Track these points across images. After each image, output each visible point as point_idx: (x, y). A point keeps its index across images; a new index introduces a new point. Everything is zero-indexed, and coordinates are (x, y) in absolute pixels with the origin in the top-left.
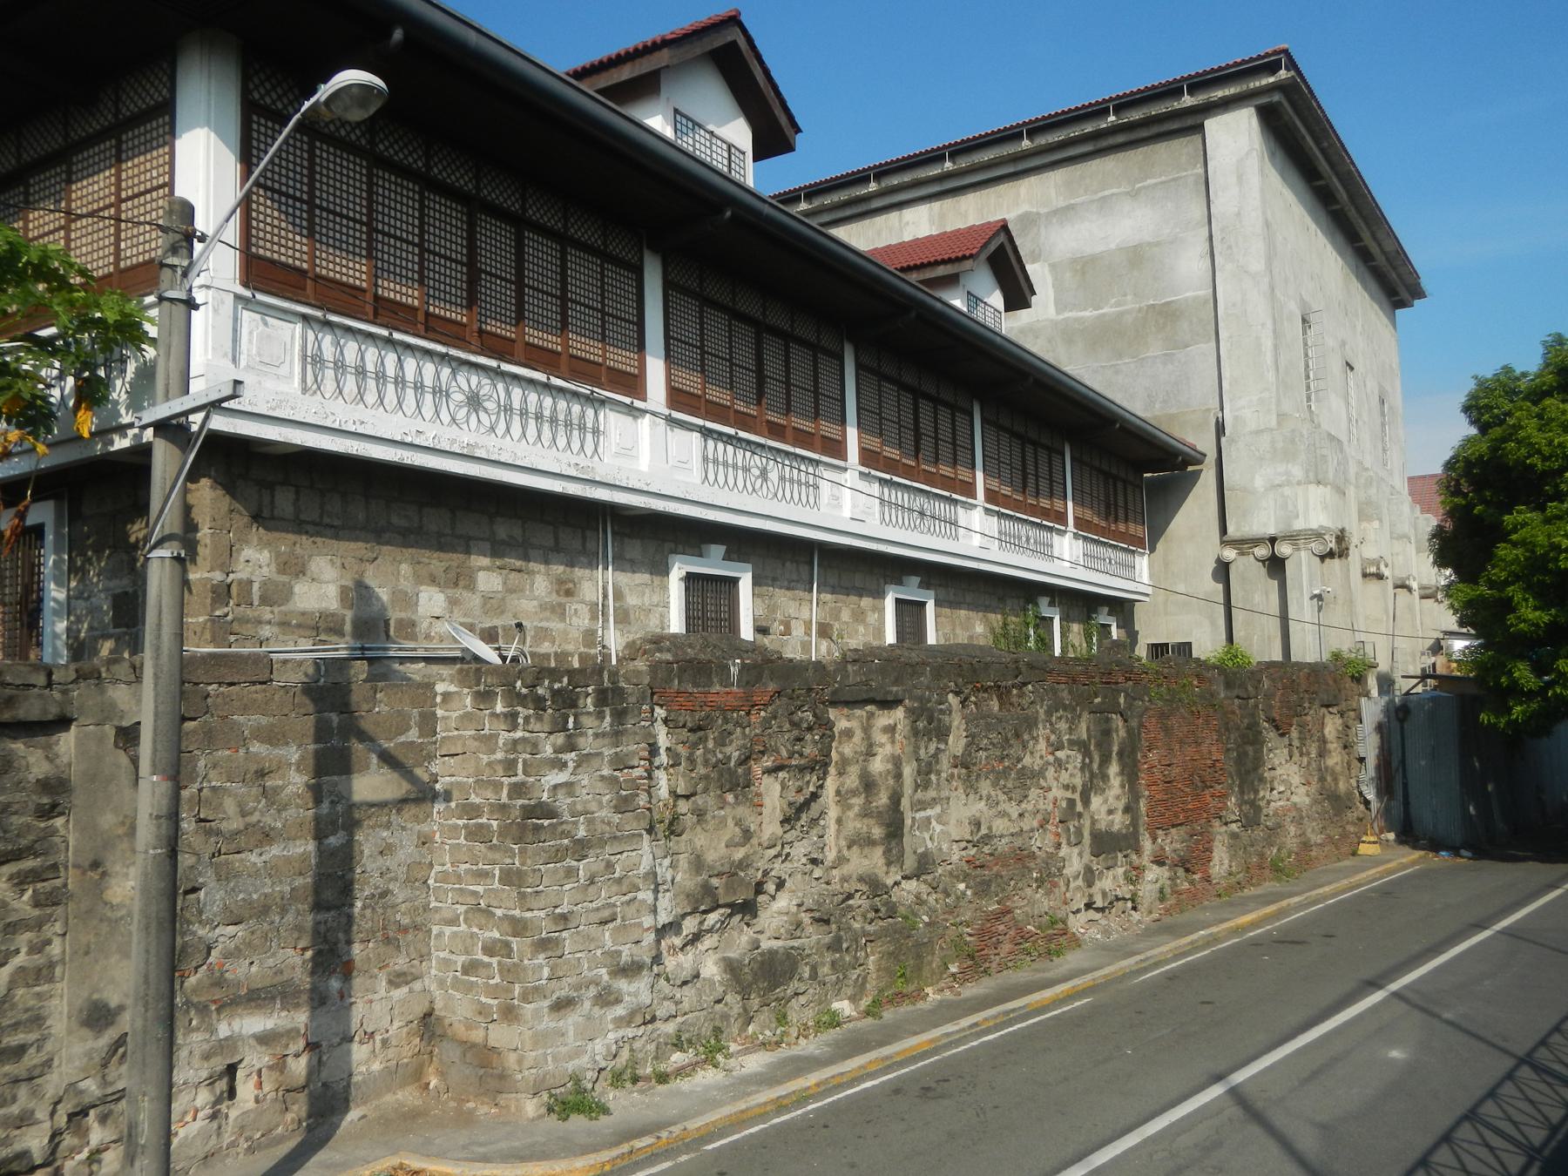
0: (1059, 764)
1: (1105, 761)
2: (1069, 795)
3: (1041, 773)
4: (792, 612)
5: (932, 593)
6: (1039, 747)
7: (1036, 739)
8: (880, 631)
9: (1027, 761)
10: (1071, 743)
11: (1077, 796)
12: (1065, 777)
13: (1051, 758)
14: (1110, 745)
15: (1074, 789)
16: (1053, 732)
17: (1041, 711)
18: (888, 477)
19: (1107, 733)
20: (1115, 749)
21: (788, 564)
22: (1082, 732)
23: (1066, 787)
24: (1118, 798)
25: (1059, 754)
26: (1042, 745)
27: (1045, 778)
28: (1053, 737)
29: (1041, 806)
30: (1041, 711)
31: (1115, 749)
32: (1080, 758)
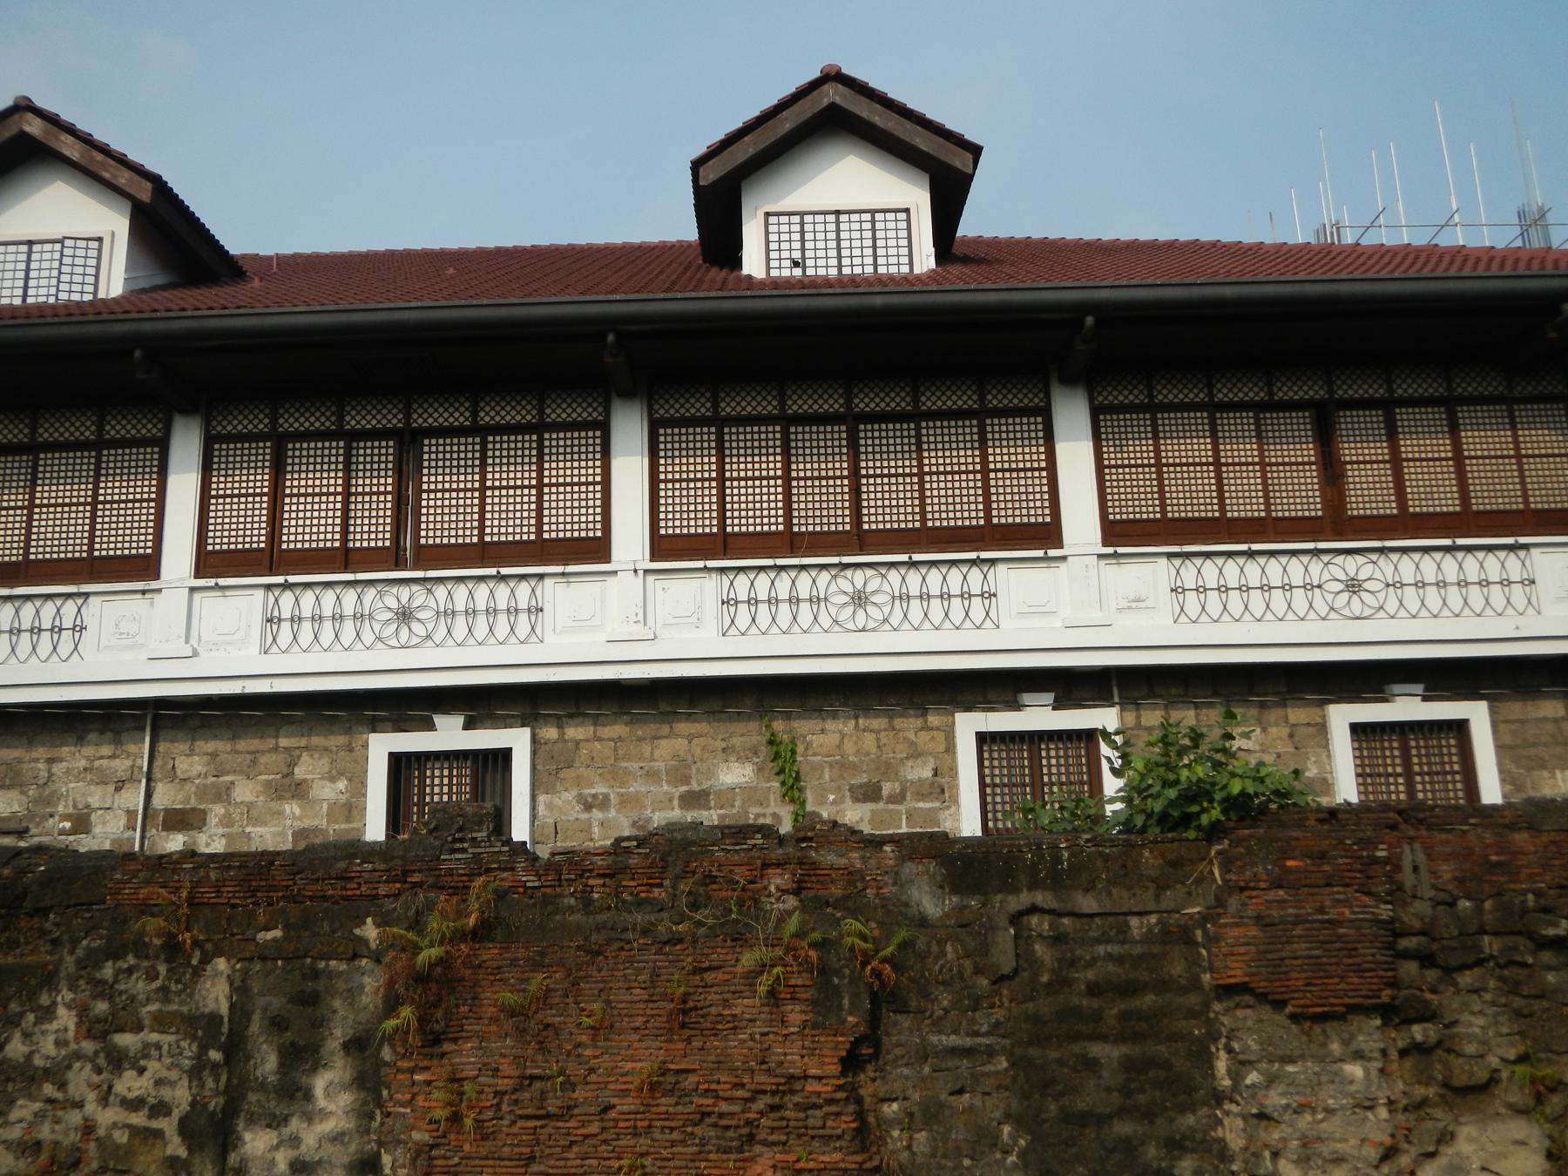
0: (118, 1061)
1: (301, 1057)
2: (138, 1119)
3: (56, 1073)
4: (94, 801)
5: (526, 733)
6: (55, 1026)
7: (48, 1013)
8: (353, 808)
9: (16, 1048)
10: (161, 1022)
11: (168, 1125)
12: (130, 1084)
13: (88, 1046)
14: (319, 1024)
15: (160, 1109)
16: (100, 996)
17: (69, 960)
18: (280, 579)
19: (309, 1001)
20: (338, 1034)
21: (93, 736)
22: (215, 993)
23: (134, 1105)
24: (337, 1138)
25: (125, 1040)
26: (66, 1019)
27: (62, 1086)
28: (101, 1007)
29: (45, 1132)
30: (69, 960)
31: (338, 1034)
32: (190, 1049)
